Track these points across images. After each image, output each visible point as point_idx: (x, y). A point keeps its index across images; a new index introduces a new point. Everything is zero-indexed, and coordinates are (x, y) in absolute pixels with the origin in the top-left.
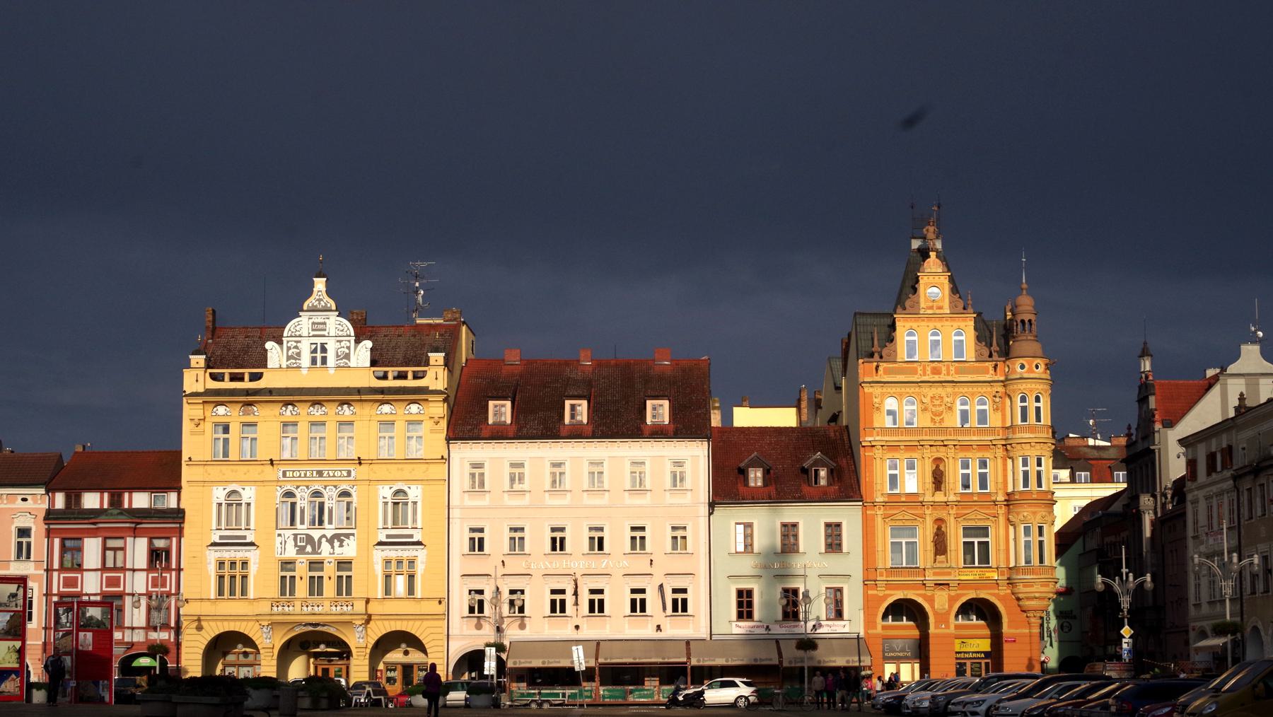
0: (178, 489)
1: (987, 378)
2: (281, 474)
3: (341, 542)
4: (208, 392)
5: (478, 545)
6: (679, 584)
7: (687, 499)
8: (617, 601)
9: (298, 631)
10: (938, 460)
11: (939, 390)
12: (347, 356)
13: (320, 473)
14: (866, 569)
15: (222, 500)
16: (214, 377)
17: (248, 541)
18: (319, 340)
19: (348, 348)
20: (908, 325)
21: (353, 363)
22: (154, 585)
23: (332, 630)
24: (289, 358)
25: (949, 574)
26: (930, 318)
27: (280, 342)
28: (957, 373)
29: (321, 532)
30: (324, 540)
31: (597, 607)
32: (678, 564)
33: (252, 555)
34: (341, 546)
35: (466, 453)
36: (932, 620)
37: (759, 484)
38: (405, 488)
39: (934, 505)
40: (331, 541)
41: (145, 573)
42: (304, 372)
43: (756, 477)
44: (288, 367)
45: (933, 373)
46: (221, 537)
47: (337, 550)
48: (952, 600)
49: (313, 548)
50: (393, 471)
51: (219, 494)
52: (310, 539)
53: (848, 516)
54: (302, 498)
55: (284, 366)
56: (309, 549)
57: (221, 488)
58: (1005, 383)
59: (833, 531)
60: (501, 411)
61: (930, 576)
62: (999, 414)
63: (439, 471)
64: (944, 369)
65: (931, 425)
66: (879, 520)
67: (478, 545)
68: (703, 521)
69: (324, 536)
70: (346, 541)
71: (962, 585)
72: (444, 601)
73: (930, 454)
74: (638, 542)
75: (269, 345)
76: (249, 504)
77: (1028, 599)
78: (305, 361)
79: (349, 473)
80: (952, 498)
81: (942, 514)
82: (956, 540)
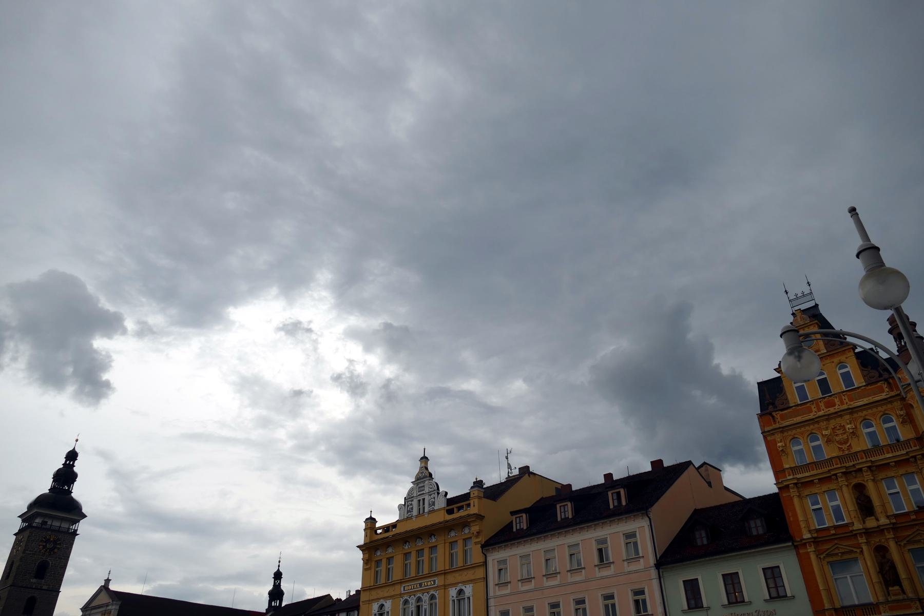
1: (883, 396)
7: (641, 564)
12: (434, 504)
13: (421, 585)
18: (421, 498)
21: (436, 508)
25: (910, 607)
28: (851, 400)
37: (705, 542)
39: (868, 533)
45: (827, 407)
59: (772, 574)
63: (480, 573)
64: (837, 401)
65: (841, 454)
66: (813, 557)
68: (655, 583)
78: (415, 513)
79: (434, 581)
80: (883, 521)
81: (876, 540)
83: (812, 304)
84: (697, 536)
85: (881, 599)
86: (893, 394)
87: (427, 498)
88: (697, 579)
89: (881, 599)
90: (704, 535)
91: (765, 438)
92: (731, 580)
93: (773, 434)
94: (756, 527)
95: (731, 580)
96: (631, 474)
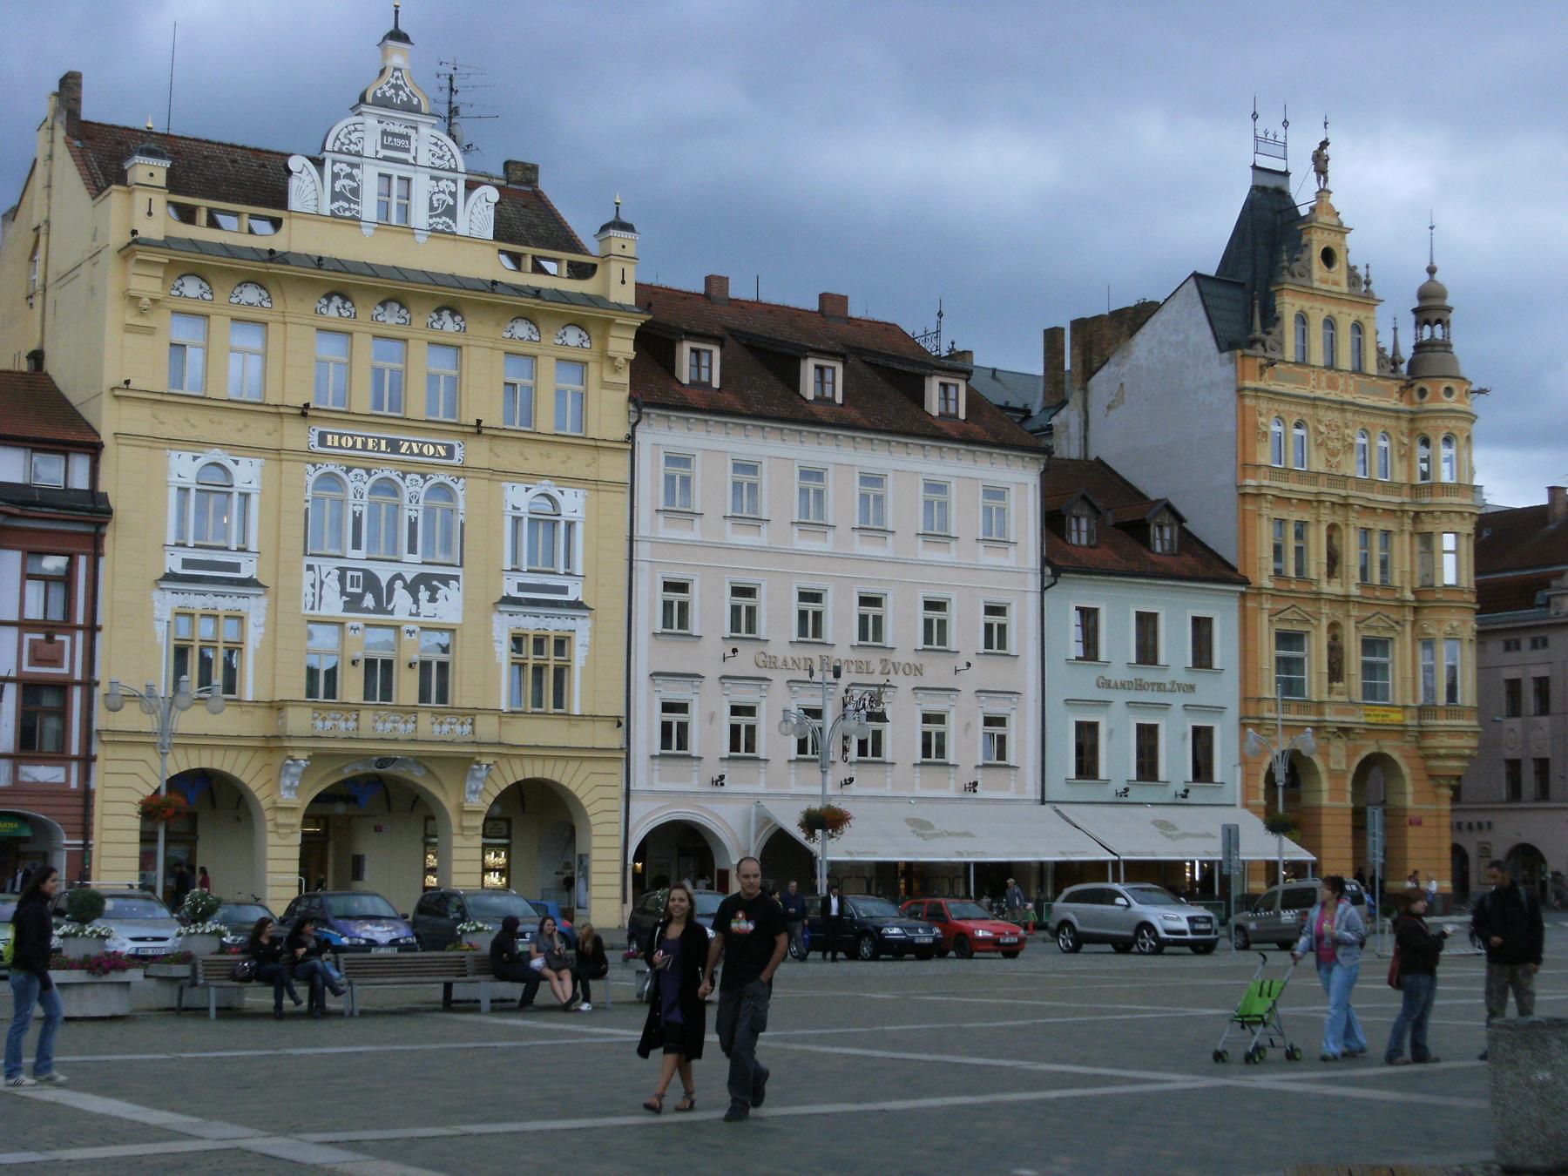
0: (94, 449)
1: (1392, 402)
2: (315, 439)
3: (433, 591)
4: (168, 243)
5: (676, 616)
6: (996, 709)
8: (709, 733)
9: (347, 773)
10: (1332, 527)
12: (451, 212)
13: (394, 445)
14: (1245, 699)
15: (190, 480)
16: (187, 215)
17: (244, 574)
19: (453, 195)
21: (461, 227)
22: (36, 660)
23: (417, 776)
24: (336, 196)
25: (1353, 713)
26: (1328, 297)
27: (318, 163)
29: (395, 568)
30: (399, 584)
31: (871, 748)
32: (991, 673)
33: (255, 608)
34: (432, 599)
35: (663, 436)
36: (1325, 785)
37: (1084, 542)
38: (554, 492)
40: (412, 588)
41: (14, 632)
42: (368, 231)
43: (1080, 532)
44: (333, 215)
45: (1329, 387)
46: (187, 563)
47: (426, 607)
48: (1349, 756)
49: (378, 599)
50: (533, 458)
51: (184, 467)
52: (371, 581)
53: (1221, 608)
54: (358, 494)
55: (327, 207)
56: (369, 600)
57: (187, 456)
58: (1414, 418)
59: (1202, 627)
60: (700, 364)
61: (1330, 716)
62: (1405, 463)
63: (615, 467)
64: (1341, 381)
67: (676, 616)
68: (1033, 601)
69: (399, 576)
70: (443, 591)
71: (1372, 730)
72: (624, 723)
73: (1327, 517)
74: (935, 633)
75: (295, 163)
76: (245, 496)
77: (1447, 757)
78: (368, 208)
79: (450, 451)
80: (1354, 591)
81: (1339, 615)
82: (1354, 659)
83: (1279, 165)
84: (1074, 526)
86: (1402, 406)
87: (422, 186)
88: (1155, 615)
89: (1325, 697)
90: (1084, 526)
92: (1147, 622)
93: (1257, 397)
95: (1147, 622)
96: (764, 298)
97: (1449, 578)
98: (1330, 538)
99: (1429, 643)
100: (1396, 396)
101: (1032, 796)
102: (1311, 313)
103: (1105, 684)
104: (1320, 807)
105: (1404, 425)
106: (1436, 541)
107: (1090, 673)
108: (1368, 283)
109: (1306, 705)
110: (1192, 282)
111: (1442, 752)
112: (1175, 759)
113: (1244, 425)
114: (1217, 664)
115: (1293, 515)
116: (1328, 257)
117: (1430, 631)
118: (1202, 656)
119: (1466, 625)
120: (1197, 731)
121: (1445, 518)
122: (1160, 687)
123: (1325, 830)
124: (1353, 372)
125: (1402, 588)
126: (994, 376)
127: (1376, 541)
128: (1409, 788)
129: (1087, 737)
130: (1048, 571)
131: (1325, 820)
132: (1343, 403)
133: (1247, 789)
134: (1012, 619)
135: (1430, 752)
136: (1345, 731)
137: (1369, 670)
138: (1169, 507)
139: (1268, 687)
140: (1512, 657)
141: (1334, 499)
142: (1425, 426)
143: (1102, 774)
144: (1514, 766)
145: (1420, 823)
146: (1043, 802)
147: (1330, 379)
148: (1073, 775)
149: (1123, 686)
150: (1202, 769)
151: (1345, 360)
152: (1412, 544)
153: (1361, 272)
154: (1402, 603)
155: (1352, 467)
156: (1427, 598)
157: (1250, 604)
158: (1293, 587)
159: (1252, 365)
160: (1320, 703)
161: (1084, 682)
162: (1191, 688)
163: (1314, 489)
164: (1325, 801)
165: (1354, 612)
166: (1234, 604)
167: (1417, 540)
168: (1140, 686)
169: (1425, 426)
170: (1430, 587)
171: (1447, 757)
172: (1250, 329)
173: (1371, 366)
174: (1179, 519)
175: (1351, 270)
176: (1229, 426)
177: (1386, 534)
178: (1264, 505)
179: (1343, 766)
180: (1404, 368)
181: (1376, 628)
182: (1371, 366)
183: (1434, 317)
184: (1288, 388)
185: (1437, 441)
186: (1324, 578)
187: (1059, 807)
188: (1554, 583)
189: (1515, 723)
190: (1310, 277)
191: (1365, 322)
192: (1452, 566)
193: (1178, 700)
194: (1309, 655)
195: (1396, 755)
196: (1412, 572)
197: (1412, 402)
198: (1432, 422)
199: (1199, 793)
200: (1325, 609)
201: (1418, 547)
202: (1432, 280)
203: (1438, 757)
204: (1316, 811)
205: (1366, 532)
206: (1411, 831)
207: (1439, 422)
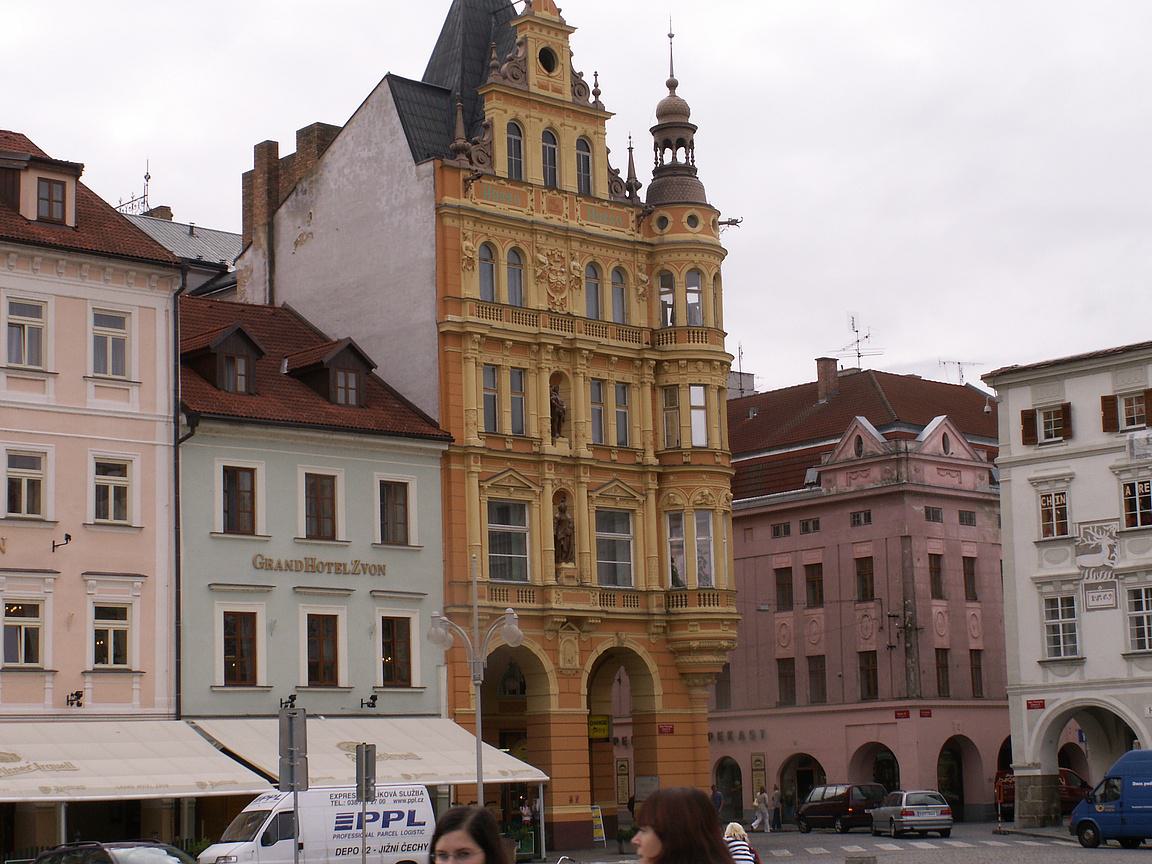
6: (112, 596)
7: (128, 404)
11: (558, 246)
14: (449, 584)
20: (513, 111)
26: (546, 104)
28: (584, 217)
32: (110, 550)
36: (554, 688)
43: (238, 376)
45: (551, 210)
58: (652, 251)
59: (393, 494)
62: (644, 304)
64: (566, 204)
68: (163, 459)
71: (607, 622)
73: (550, 364)
77: (701, 650)
80: (585, 453)
81: (568, 481)
82: (587, 536)
85: (552, 581)
86: (639, 237)
89: (552, 581)
91: (440, 216)
92: (320, 491)
93: (460, 217)
94: (347, 388)
95: (320, 491)
97: (699, 439)
98: (554, 390)
99: (676, 519)
100: (633, 226)
101: (164, 710)
102: (526, 122)
103: (266, 565)
104: (548, 715)
105: (642, 259)
106: (682, 394)
107: (241, 551)
108: (597, 93)
109: (529, 591)
110: (386, 84)
111: (695, 644)
112: (360, 657)
113: (444, 249)
114: (414, 539)
115: (509, 361)
116: (548, 59)
117: (679, 501)
118: (394, 530)
119: (720, 494)
120: (389, 624)
121: (691, 368)
122: (340, 569)
123: (554, 743)
124: (580, 194)
125: (644, 451)
126: (191, 233)
127: (611, 393)
128: (658, 690)
129: (240, 633)
130: (183, 419)
131: (554, 730)
132: (567, 230)
133: (456, 695)
134: (134, 481)
135: (680, 645)
136: (576, 622)
137: (608, 549)
138: (352, 349)
139: (480, 571)
140: (783, 543)
141: (559, 343)
142: (664, 261)
143: (262, 678)
144: (786, 665)
145: (672, 731)
146: (178, 716)
147: (551, 201)
148: (220, 679)
149: (289, 567)
150: (397, 673)
151: (569, 180)
152: (654, 400)
153: (588, 79)
154: (642, 470)
155: (579, 306)
156: (673, 463)
157: (455, 466)
158: (509, 446)
159: (454, 180)
160: (546, 587)
161: (235, 559)
162: (380, 570)
163: (534, 330)
164: (554, 707)
165: (586, 478)
166: (434, 469)
167: (660, 395)
168: (312, 567)
169: (664, 261)
170: (678, 450)
171: (701, 650)
172: (451, 134)
173: (601, 189)
174: (369, 365)
175: (577, 77)
176: (428, 252)
177: (624, 387)
178: (470, 346)
179: (577, 663)
180: (642, 195)
181: (613, 498)
182: (601, 189)
183: (674, 136)
184: (500, 208)
185: (680, 279)
186: (548, 437)
187: (199, 723)
188: (825, 459)
189: (787, 617)
190: (526, 79)
191: (595, 138)
192: (700, 428)
193: (362, 584)
194: (530, 530)
195: (640, 651)
196: (655, 433)
197: (651, 233)
198: (675, 256)
199: (389, 700)
200: (550, 474)
201: (661, 403)
202: (673, 94)
203: (690, 651)
204: (544, 719)
205: (599, 384)
206: (661, 741)
207: (683, 256)
